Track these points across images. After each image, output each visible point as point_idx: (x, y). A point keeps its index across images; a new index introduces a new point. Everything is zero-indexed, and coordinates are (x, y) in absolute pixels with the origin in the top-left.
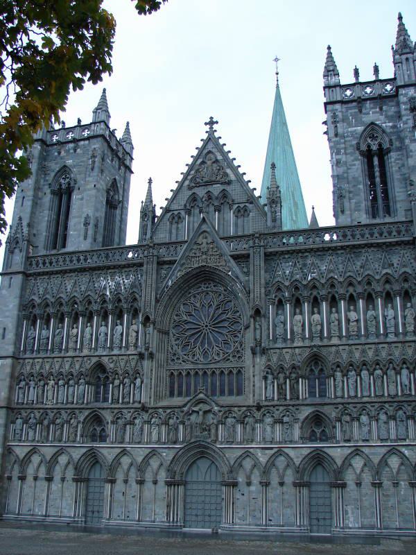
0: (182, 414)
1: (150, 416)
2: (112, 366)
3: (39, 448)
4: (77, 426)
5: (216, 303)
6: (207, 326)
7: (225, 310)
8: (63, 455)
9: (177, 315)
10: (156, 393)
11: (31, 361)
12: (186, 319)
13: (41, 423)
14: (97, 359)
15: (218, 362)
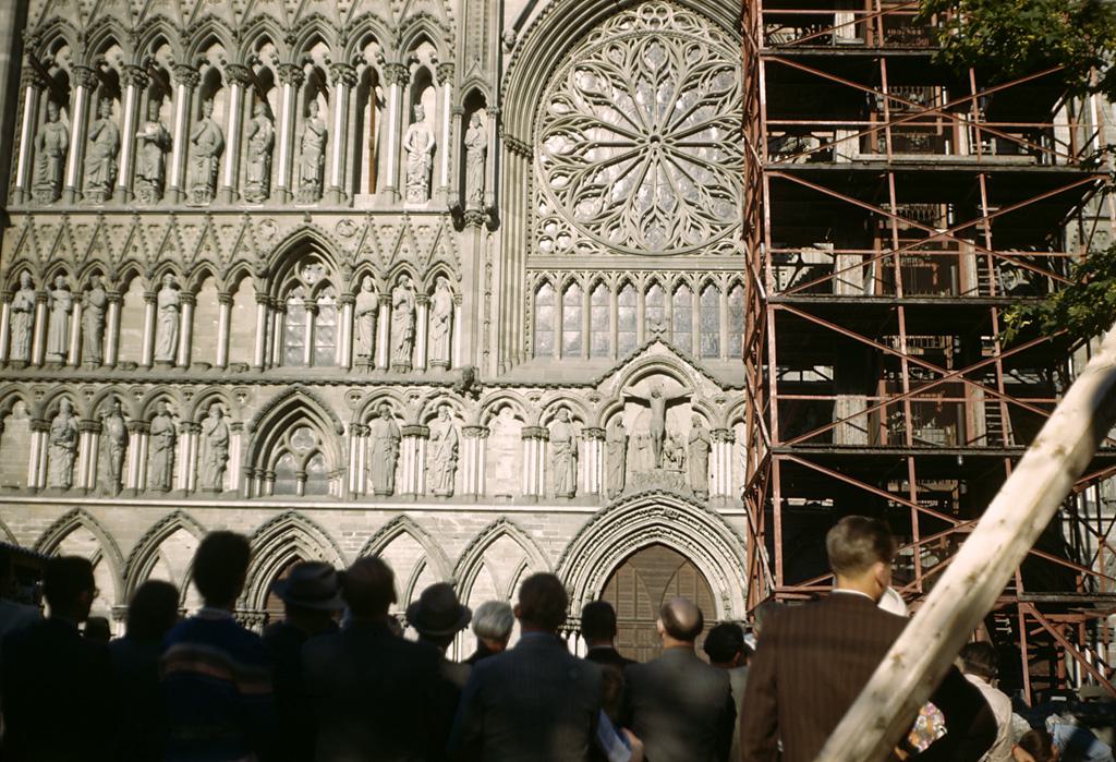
0: (596, 407)
1: (487, 411)
2: (351, 245)
3: (89, 510)
4: (225, 443)
5: (684, 73)
6: (654, 139)
7: (711, 96)
8: (179, 534)
9: (555, 101)
10: (501, 337)
11: (57, 221)
12: (589, 113)
13: (96, 428)
14: (299, 221)
15: (696, 251)
